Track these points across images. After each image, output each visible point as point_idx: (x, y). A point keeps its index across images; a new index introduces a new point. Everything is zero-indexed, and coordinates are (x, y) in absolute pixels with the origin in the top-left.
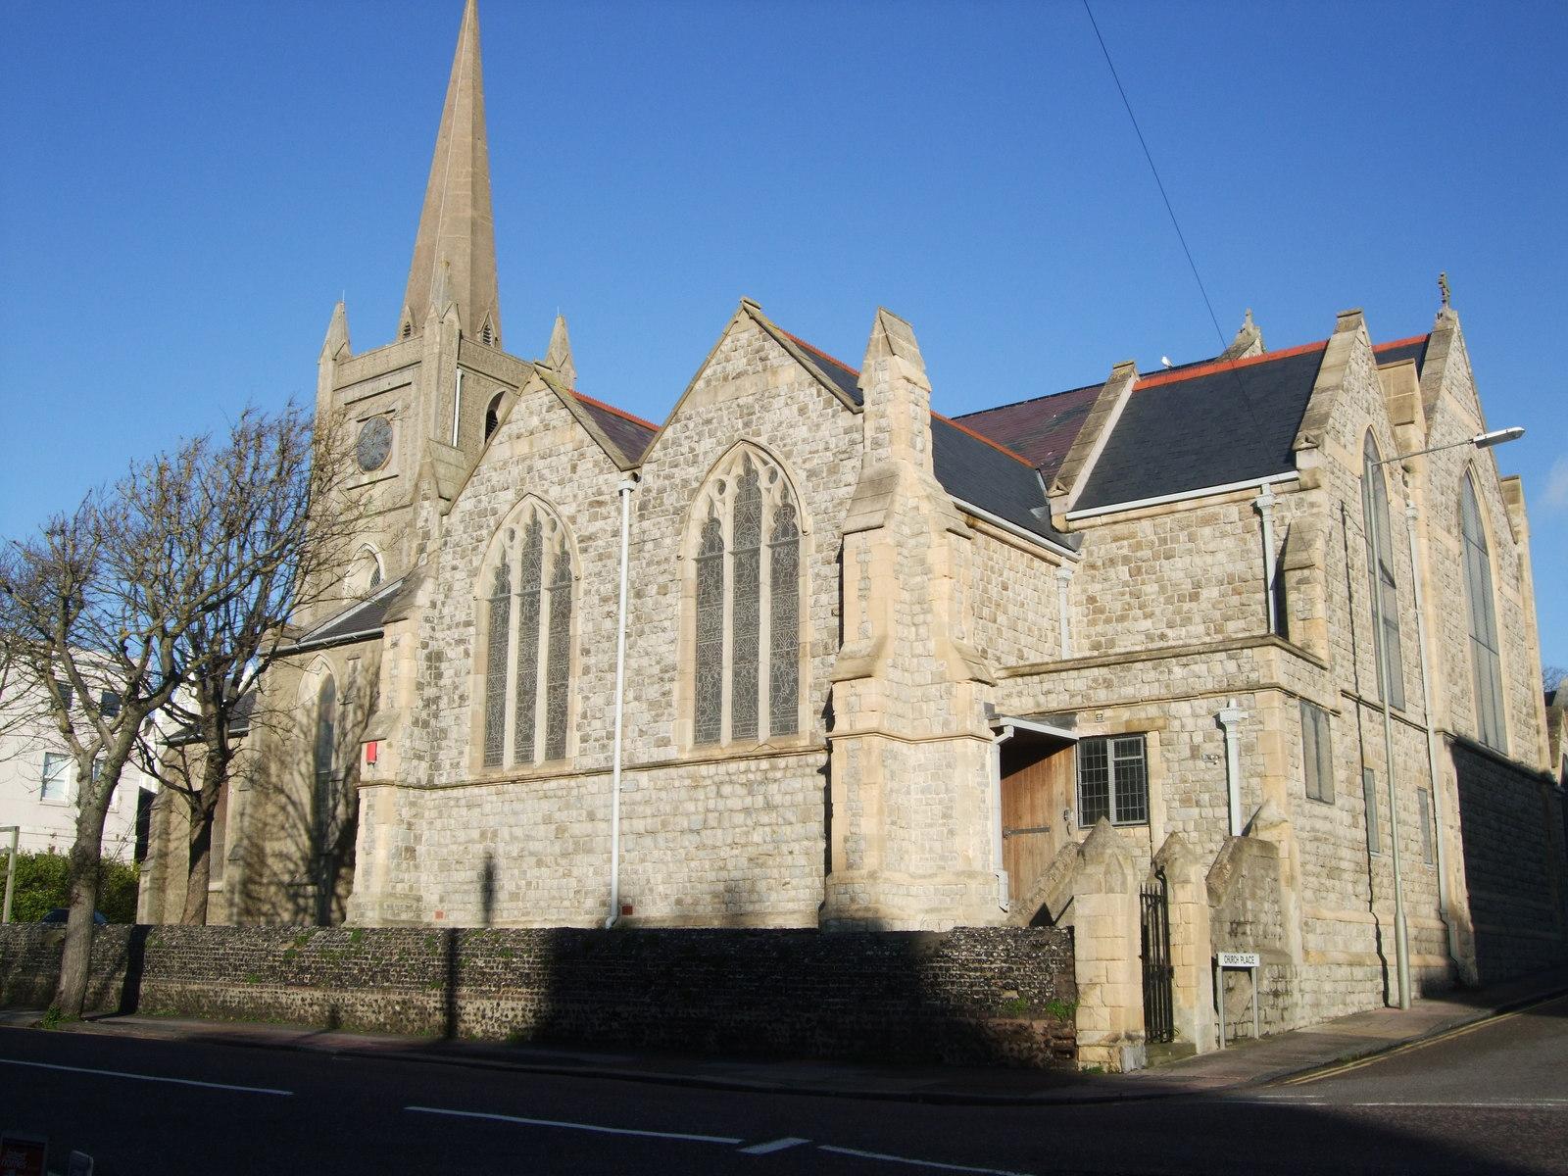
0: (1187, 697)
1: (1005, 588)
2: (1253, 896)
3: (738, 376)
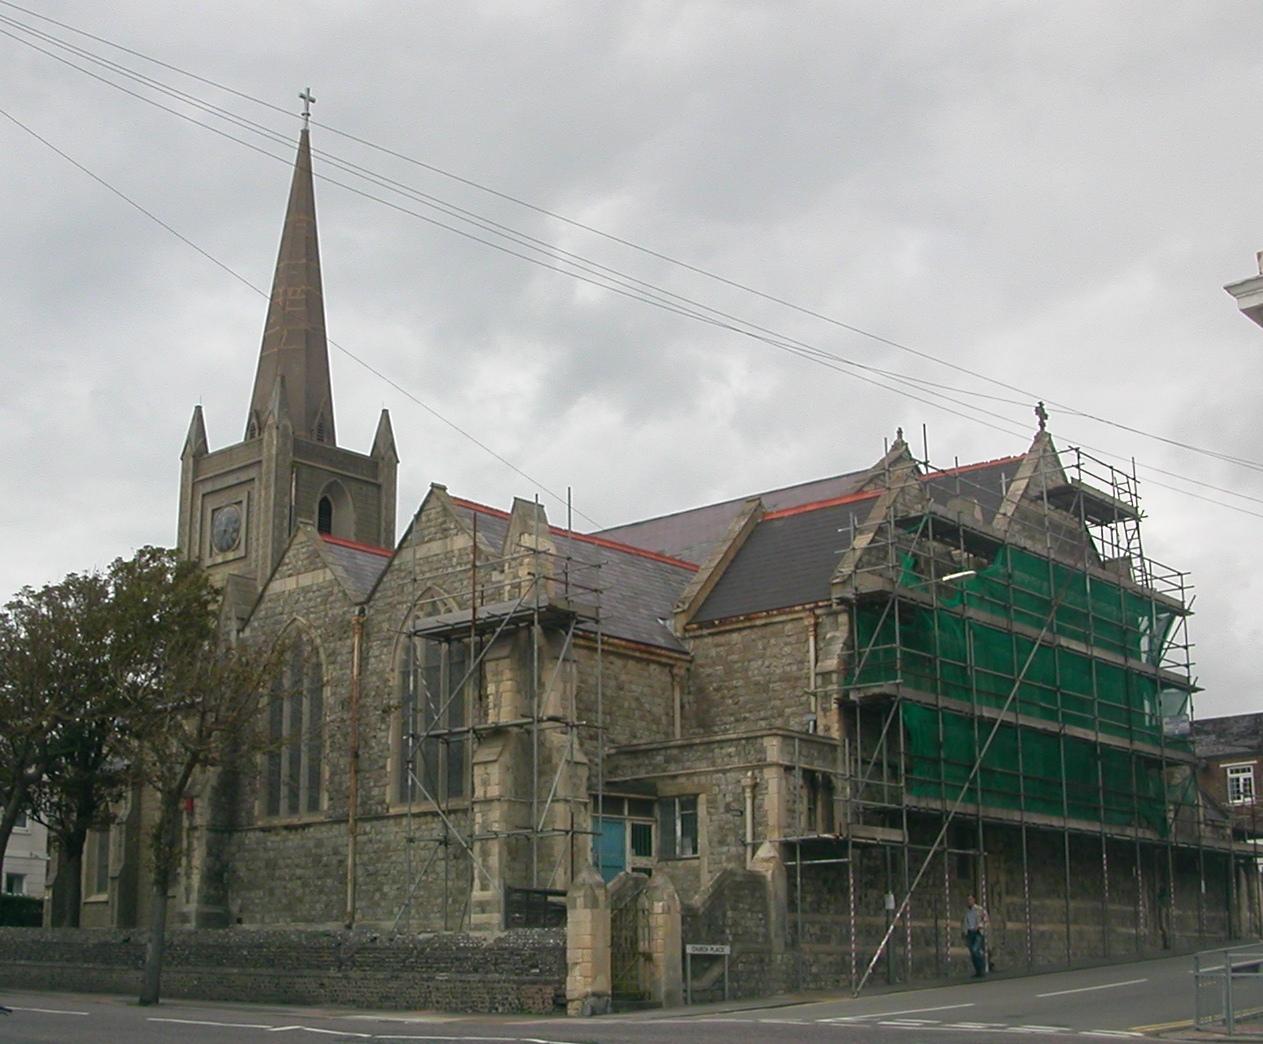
0: (724, 772)
1: (621, 689)
2: (734, 909)
3: (430, 540)
